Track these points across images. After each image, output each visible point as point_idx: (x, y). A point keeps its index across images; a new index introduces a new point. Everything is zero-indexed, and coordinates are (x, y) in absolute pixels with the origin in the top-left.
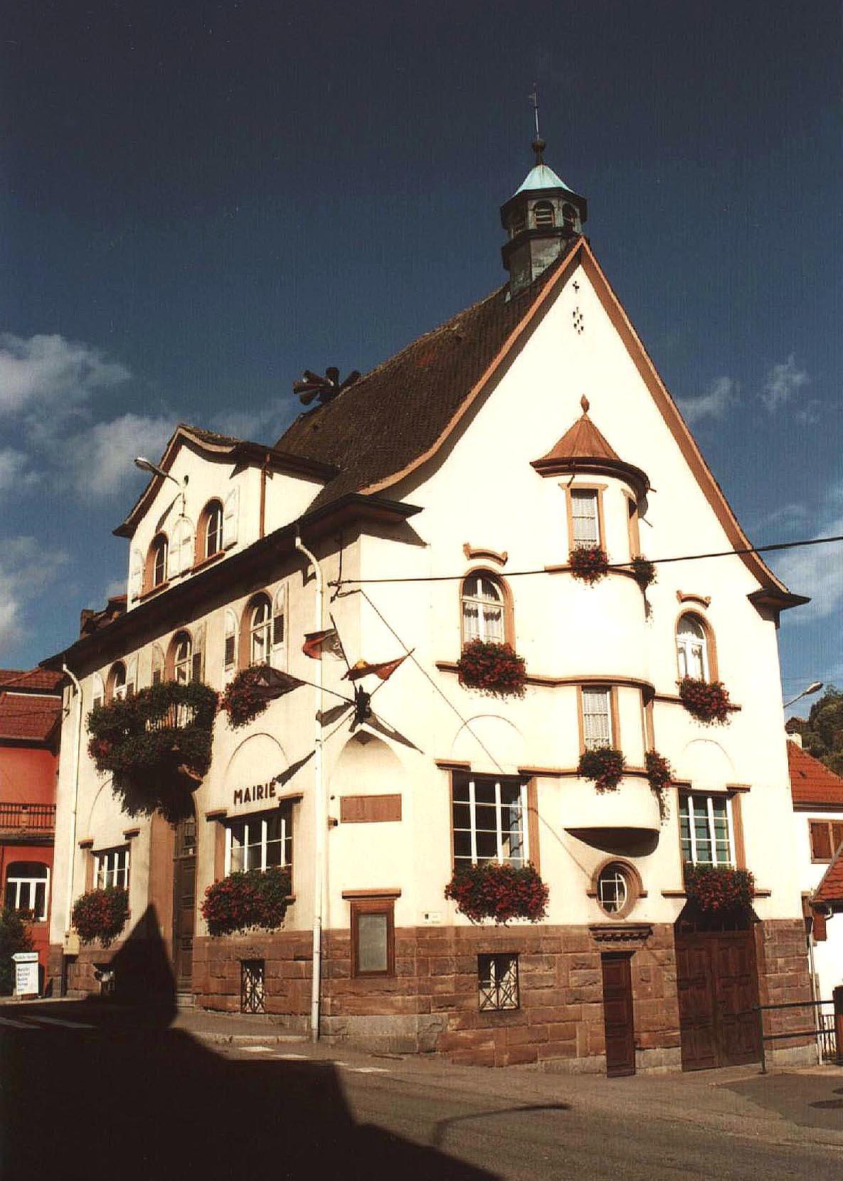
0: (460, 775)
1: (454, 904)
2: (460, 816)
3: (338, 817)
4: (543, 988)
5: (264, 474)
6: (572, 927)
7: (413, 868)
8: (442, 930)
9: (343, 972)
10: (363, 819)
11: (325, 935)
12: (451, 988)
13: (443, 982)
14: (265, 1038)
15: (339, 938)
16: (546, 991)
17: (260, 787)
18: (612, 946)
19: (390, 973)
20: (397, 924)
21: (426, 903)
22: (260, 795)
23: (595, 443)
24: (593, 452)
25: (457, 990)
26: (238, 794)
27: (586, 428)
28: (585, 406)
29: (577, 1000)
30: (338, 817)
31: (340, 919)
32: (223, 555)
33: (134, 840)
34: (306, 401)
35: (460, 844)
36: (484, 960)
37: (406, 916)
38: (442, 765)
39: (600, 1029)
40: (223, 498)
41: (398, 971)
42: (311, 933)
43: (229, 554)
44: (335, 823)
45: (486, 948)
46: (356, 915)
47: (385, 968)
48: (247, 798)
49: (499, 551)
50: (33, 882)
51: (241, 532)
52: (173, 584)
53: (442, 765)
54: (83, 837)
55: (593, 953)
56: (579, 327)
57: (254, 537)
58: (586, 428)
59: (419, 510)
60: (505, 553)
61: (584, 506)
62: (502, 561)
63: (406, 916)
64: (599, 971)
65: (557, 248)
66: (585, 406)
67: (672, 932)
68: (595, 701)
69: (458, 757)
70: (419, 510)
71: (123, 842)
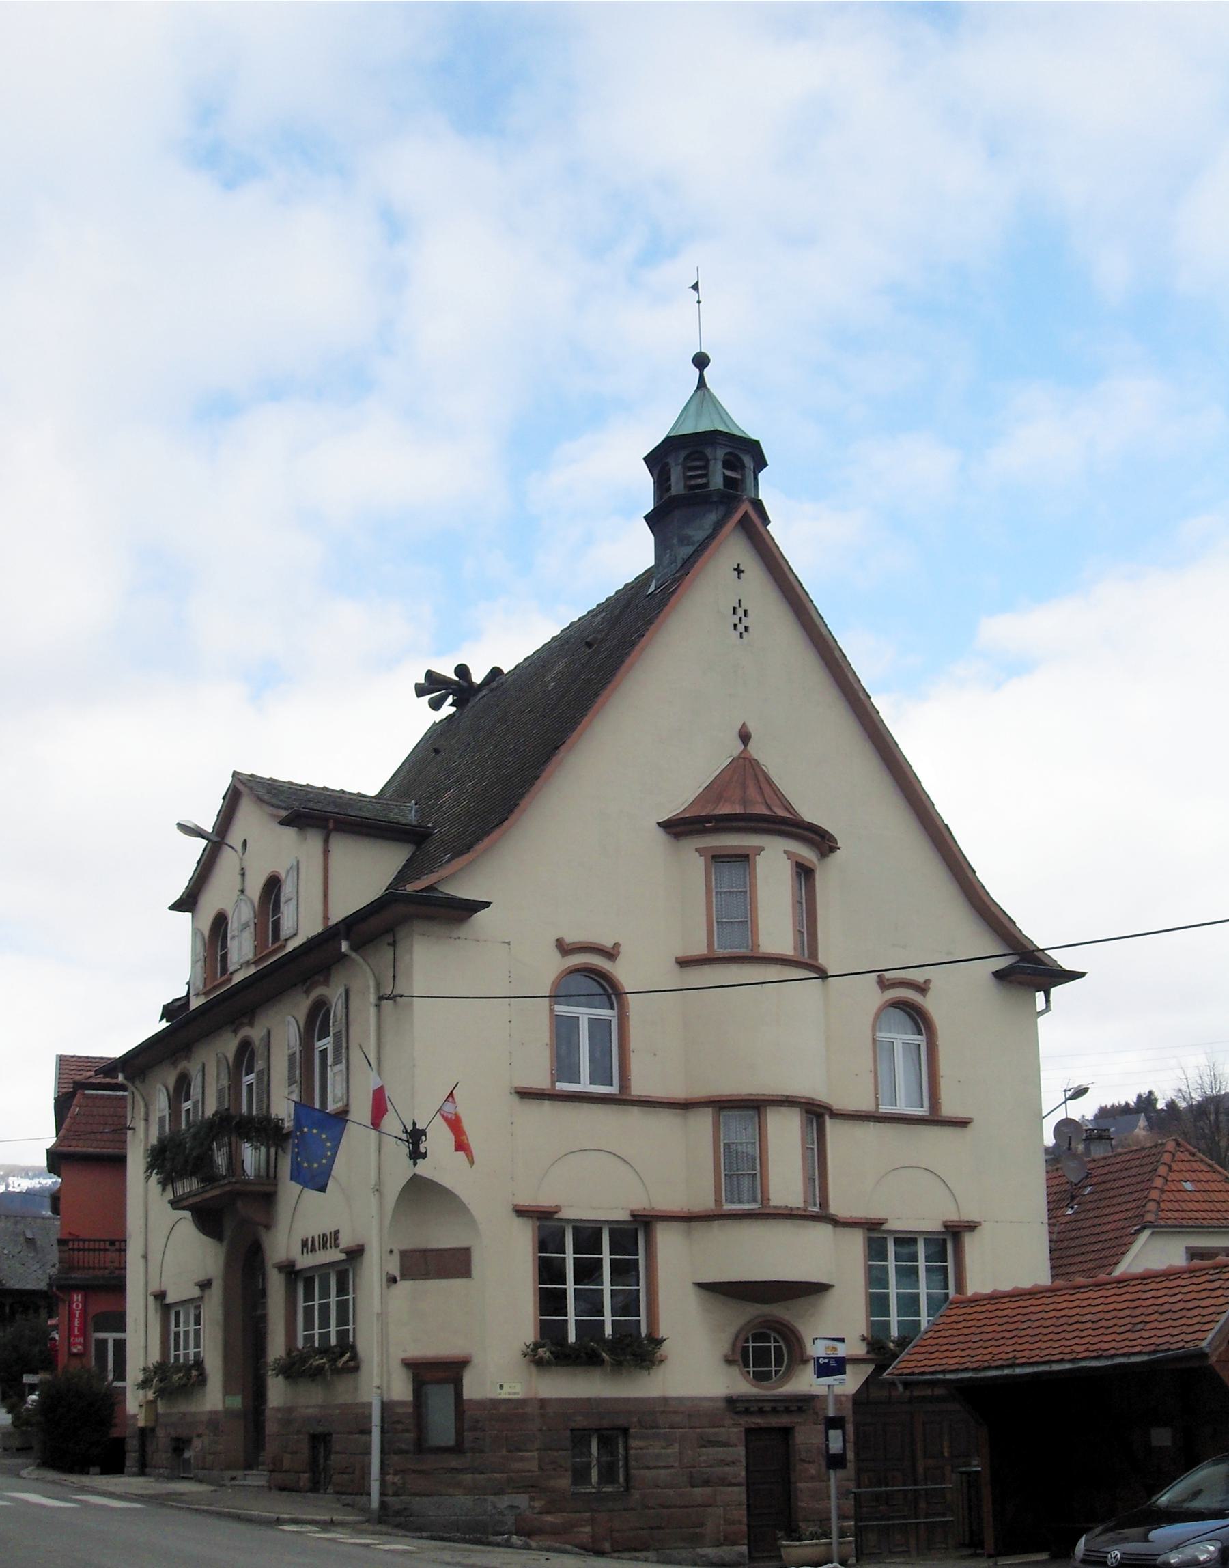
0: (546, 1226)
1: (735, 1371)
2: (549, 1271)
3: (397, 1274)
4: (659, 1467)
5: (326, 841)
6: (706, 1399)
7: (492, 1329)
8: (523, 1402)
9: (403, 1446)
10: (426, 1276)
11: (386, 1407)
12: (534, 1466)
13: (522, 1459)
14: (318, 1518)
15: (400, 1410)
16: (662, 1471)
17: (324, 1235)
18: (759, 1421)
19: (458, 1449)
20: (466, 1395)
21: (501, 1372)
22: (325, 1247)
23: (752, 792)
24: (744, 802)
25: (540, 1468)
26: (304, 1244)
27: (745, 771)
28: (745, 737)
29: (706, 1483)
30: (397, 1274)
31: (401, 1390)
32: (230, 980)
33: (207, 1293)
34: (436, 705)
35: (551, 1302)
36: (580, 1438)
37: (476, 1387)
38: (521, 1212)
39: (741, 1514)
40: (283, 875)
41: (467, 1445)
42: (370, 1405)
43: (291, 946)
44: (393, 1280)
45: (580, 1421)
46: (419, 1386)
47: (452, 1443)
48: (313, 1250)
49: (608, 943)
50: (111, 1337)
51: (302, 922)
52: (237, 979)
53: (521, 1212)
54: (154, 1287)
55: (734, 1431)
56: (741, 628)
57: (318, 929)
58: (745, 771)
59: (486, 905)
60: (617, 945)
61: (730, 876)
62: (611, 954)
63: (476, 1387)
64: (741, 1451)
65: (713, 517)
66: (745, 737)
67: (850, 1405)
68: (739, 1129)
69: (545, 1200)
70: (486, 905)
71: (196, 1292)
